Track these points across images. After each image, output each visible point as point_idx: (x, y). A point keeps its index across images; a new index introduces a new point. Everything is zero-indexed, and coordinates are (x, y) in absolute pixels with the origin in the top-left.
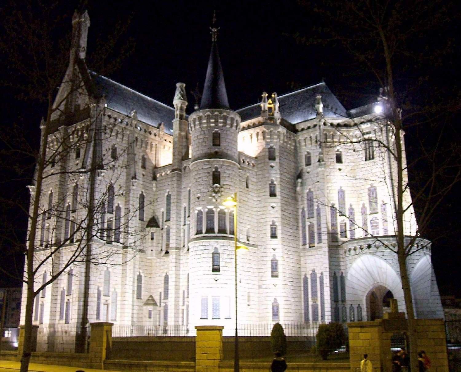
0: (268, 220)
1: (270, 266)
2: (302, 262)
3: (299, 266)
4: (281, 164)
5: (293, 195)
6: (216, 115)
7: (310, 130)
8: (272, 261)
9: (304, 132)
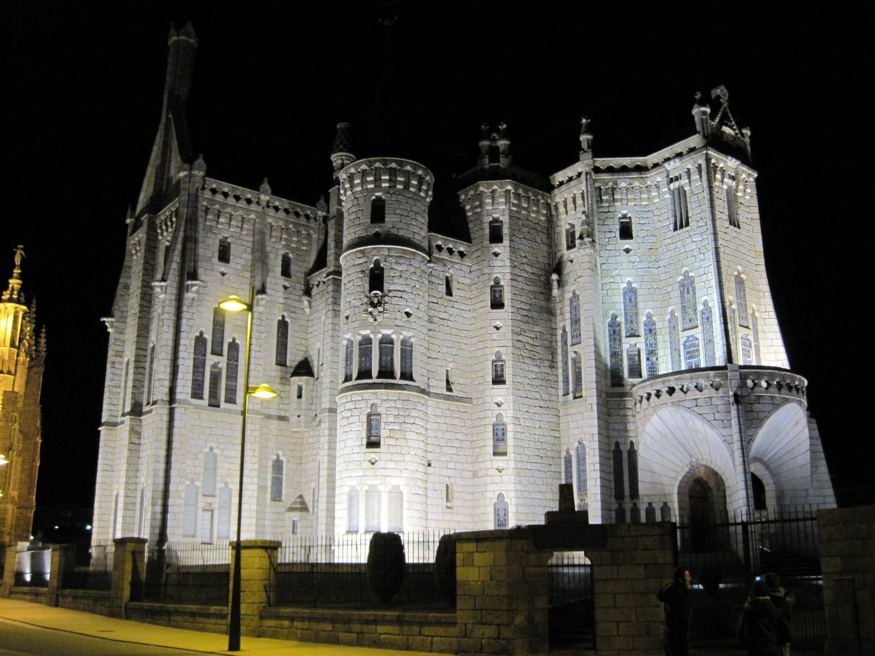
0: (488, 351)
1: (490, 435)
3: (556, 434)
4: (513, 250)
5: (544, 304)
6: (376, 168)
7: (572, 183)
8: (494, 426)
9: (563, 187)
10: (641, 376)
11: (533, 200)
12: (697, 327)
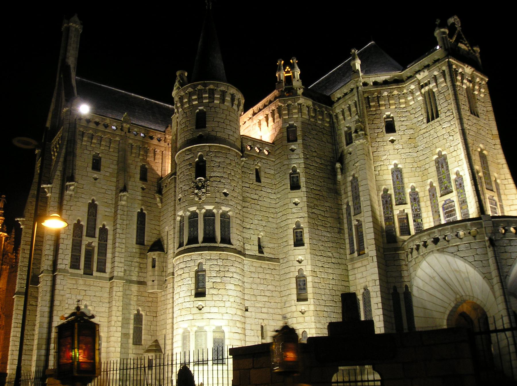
0: (289, 221)
1: (294, 285)
2: (351, 278)
3: (346, 284)
4: (305, 146)
5: (331, 186)
6: (199, 90)
7: (347, 97)
8: (297, 278)
9: (341, 101)
10: (410, 234)
11: (319, 111)
12: (452, 192)
